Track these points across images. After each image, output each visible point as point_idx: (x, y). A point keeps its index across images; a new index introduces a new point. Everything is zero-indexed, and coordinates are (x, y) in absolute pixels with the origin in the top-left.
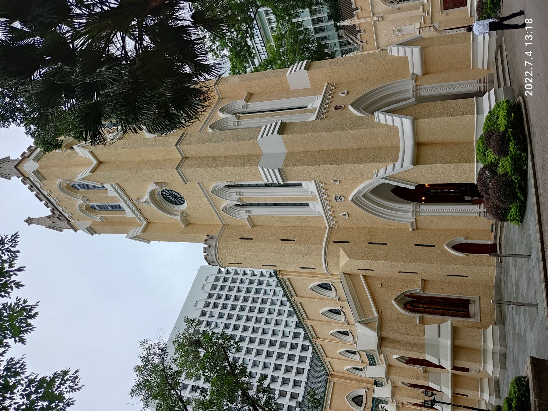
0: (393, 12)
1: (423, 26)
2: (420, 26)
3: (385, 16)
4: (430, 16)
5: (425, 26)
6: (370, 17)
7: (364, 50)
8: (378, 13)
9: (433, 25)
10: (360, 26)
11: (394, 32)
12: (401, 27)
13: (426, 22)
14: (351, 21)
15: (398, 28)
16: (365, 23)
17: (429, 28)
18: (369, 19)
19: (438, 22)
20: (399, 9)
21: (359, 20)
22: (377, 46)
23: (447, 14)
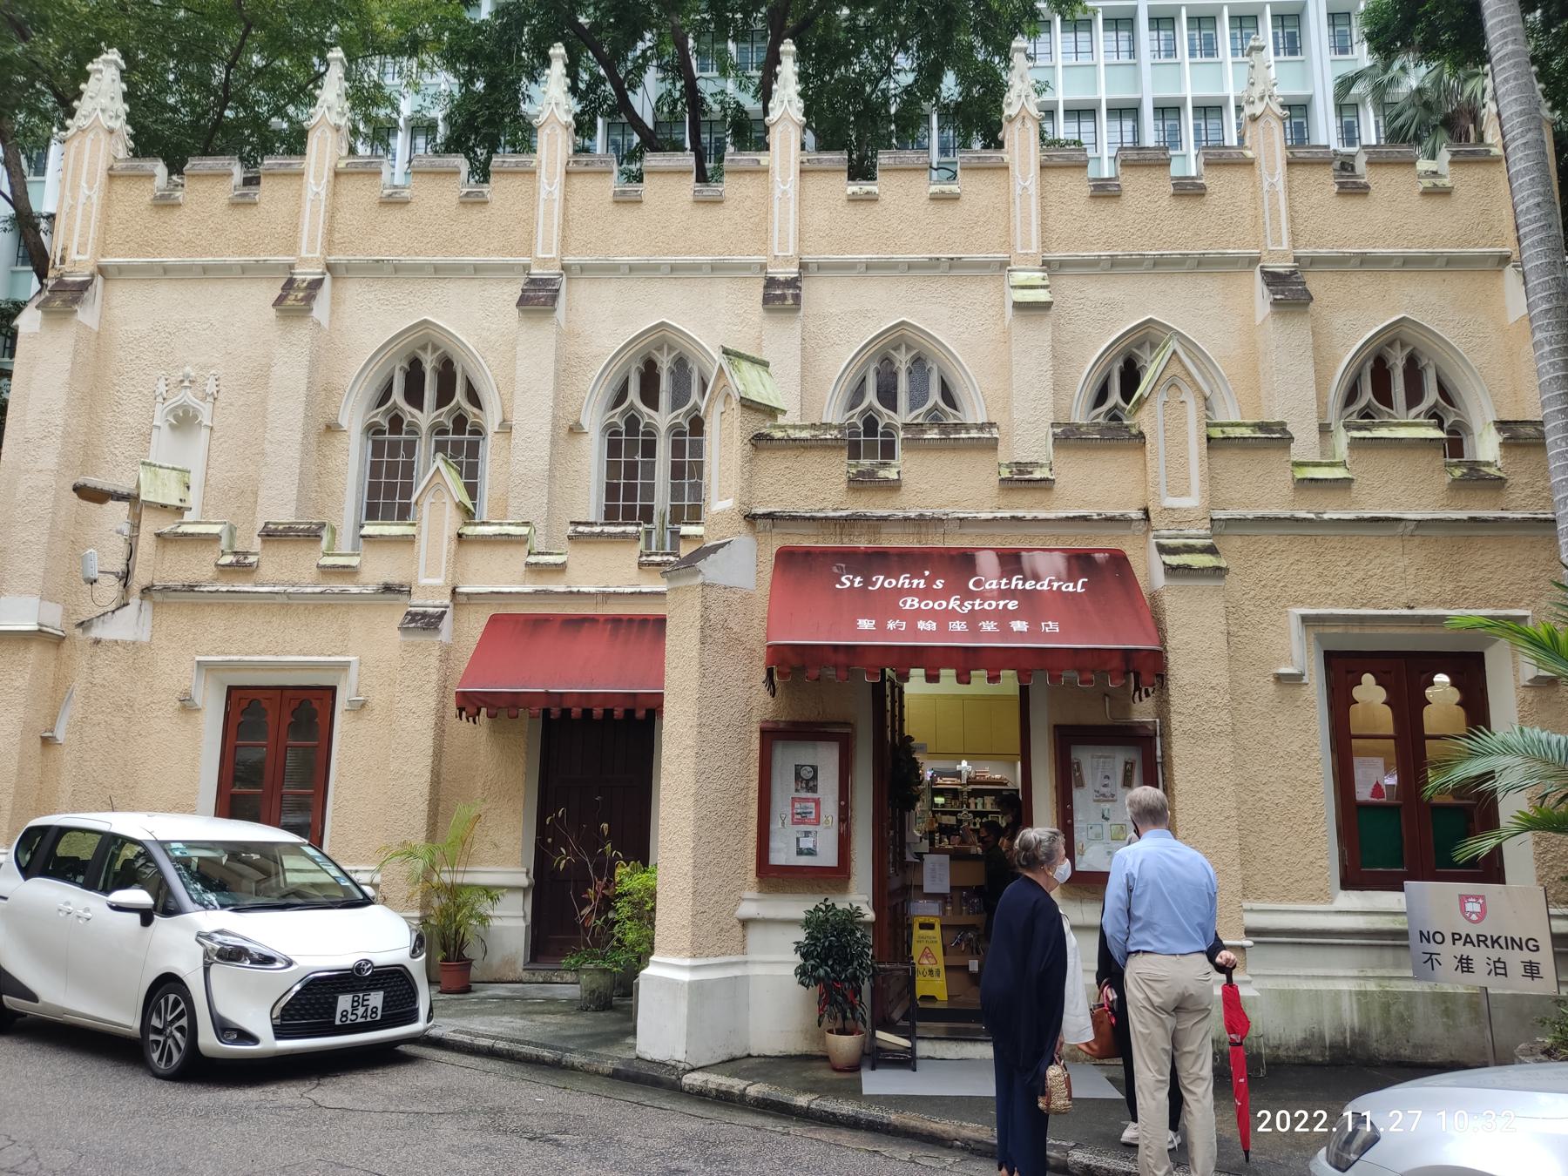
0: (320, 393)
1: (151, 525)
2: (151, 506)
3: (302, 334)
4: (216, 580)
5: (146, 543)
6: (330, 244)
7: (119, 187)
8: (335, 302)
9: (134, 601)
10: (286, 181)
11: (186, 382)
12: (205, 433)
13: (172, 554)
14: (338, 129)
15: (205, 414)
16: (297, 214)
17: (120, 567)
18: (312, 241)
19: (145, 638)
20: (332, 428)
21: (327, 174)
22: (121, 269)
23: (187, 705)
